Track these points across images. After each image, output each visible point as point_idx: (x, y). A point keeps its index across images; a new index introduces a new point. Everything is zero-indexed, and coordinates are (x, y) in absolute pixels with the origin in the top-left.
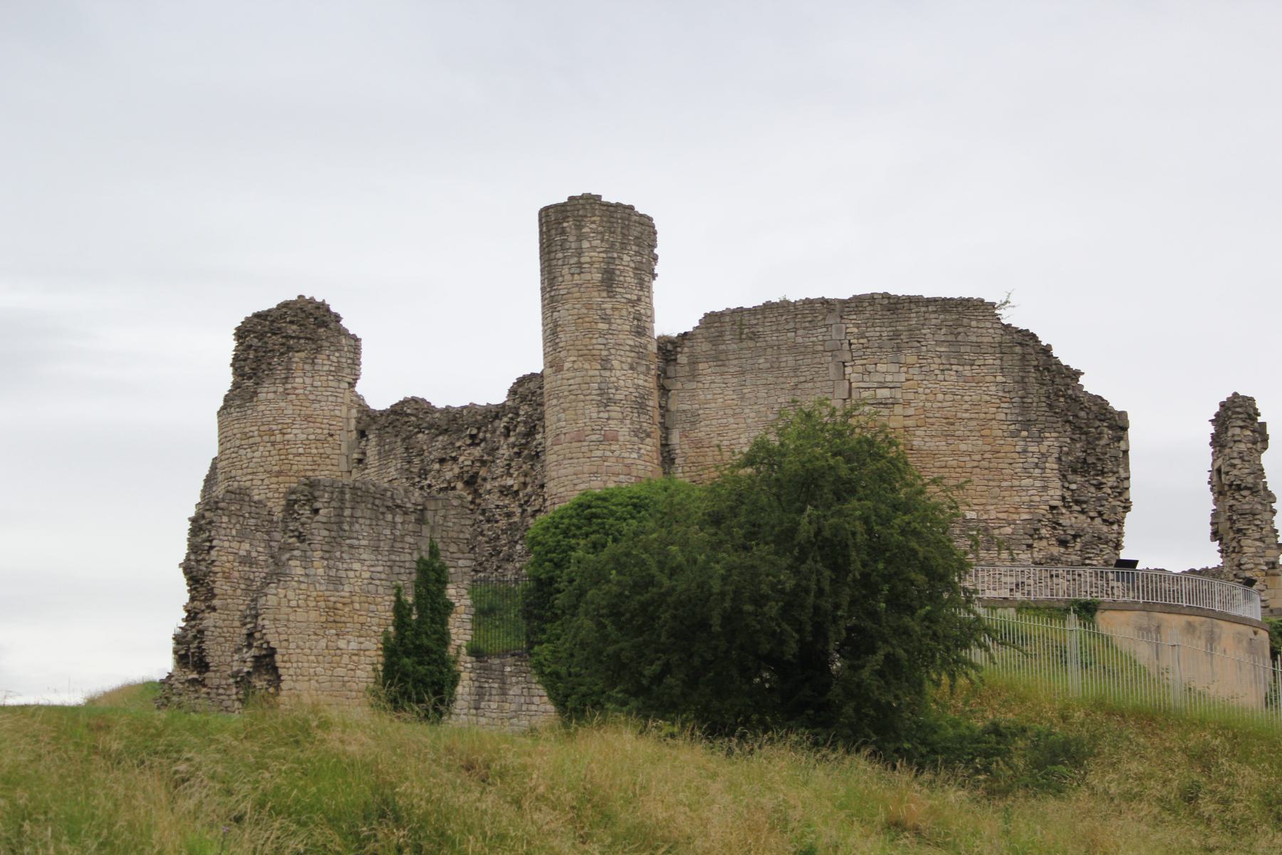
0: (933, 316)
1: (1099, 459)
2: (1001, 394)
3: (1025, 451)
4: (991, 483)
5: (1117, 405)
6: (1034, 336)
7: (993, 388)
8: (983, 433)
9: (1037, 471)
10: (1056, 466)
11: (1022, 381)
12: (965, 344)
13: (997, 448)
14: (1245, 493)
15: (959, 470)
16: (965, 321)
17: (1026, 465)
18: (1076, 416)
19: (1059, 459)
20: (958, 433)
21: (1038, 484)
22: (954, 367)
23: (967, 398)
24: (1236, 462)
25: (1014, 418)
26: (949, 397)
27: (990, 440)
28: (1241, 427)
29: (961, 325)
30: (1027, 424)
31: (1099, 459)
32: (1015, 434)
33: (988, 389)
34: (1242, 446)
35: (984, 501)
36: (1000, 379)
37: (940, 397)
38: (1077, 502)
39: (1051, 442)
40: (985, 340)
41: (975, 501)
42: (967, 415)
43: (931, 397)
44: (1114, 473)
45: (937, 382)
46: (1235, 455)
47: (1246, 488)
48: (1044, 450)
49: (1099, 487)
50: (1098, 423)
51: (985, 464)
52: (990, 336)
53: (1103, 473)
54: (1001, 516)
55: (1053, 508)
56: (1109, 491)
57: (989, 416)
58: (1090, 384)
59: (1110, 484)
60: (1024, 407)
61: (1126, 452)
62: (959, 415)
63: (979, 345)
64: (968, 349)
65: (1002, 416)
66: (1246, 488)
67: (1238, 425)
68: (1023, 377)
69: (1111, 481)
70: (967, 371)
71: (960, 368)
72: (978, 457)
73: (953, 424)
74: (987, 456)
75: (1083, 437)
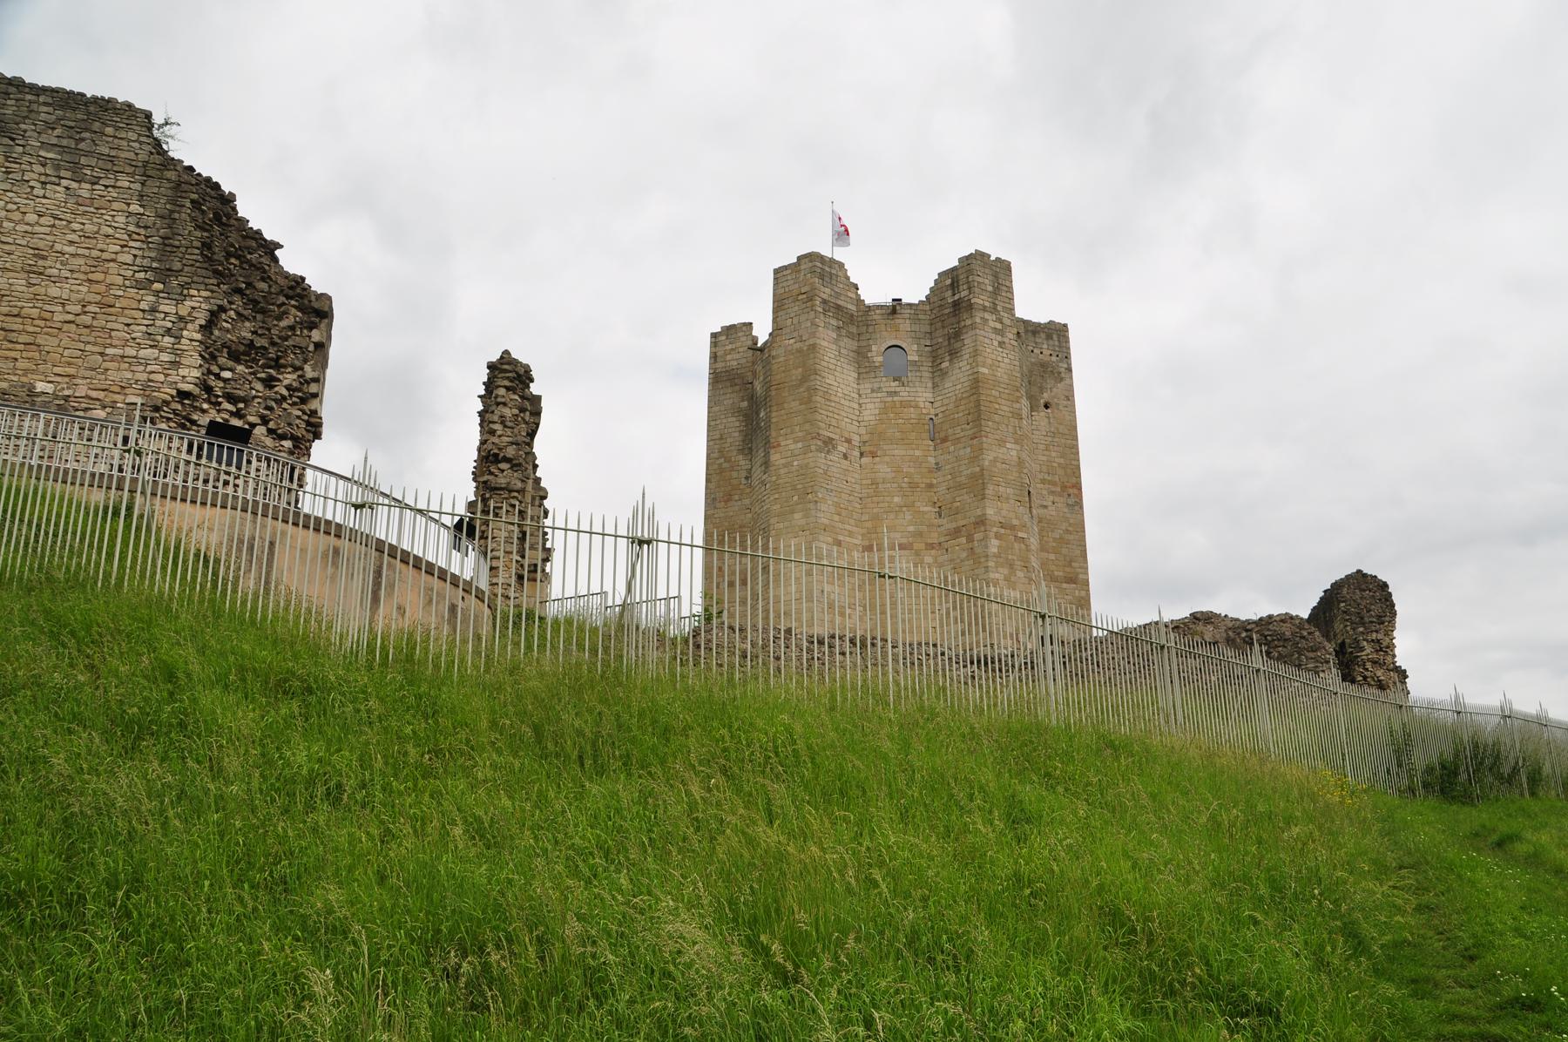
0: (45, 109)
1: (273, 344)
2: (132, 228)
3: (154, 310)
4: (89, 348)
5: (316, 284)
6: (217, 186)
7: (121, 219)
8: (91, 276)
9: (167, 339)
10: (198, 336)
11: (169, 218)
12: (88, 154)
13: (111, 300)
14: (504, 466)
15: (42, 323)
16: (96, 126)
17: (151, 330)
18: (249, 285)
19: (207, 328)
20: (49, 271)
21: (165, 357)
22: (64, 183)
23: (75, 226)
24: (497, 427)
25: (146, 262)
26: (45, 220)
27: (102, 288)
28: (508, 389)
29: (86, 130)
30: (165, 274)
31: (273, 344)
32: (141, 285)
33: (116, 221)
34: (507, 412)
35: (71, 371)
36: (135, 208)
37: (32, 218)
38: (231, 398)
39: (198, 303)
40: (123, 155)
41: (56, 370)
42: (71, 249)
43: (17, 216)
44: (296, 369)
45: (30, 195)
46: (496, 418)
47: (506, 460)
48: (183, 311)
49: (269, 382)
50: (282, 299)
51: (87, 319)
52: (132, 147)
53: (278, 366)
54: (94, 394)
55: (183, 395)
56: (285, 392)
57: (105, 256)
58: (290, 261)
59: (286, 382)
60: (167, 247)
61: (322, 347)
62: (58, 247)
63: (111, 159)
64: (93, 162)
65: (128, 258)
66: (506, 460)
67: (510, 392)
68: (172, 212)
69: (289, 378)
70: (84, 190)
71: (74, 185)
72: (78, 309)
73: (44, 258)
74: (91, 308)
75: (259, 317)
